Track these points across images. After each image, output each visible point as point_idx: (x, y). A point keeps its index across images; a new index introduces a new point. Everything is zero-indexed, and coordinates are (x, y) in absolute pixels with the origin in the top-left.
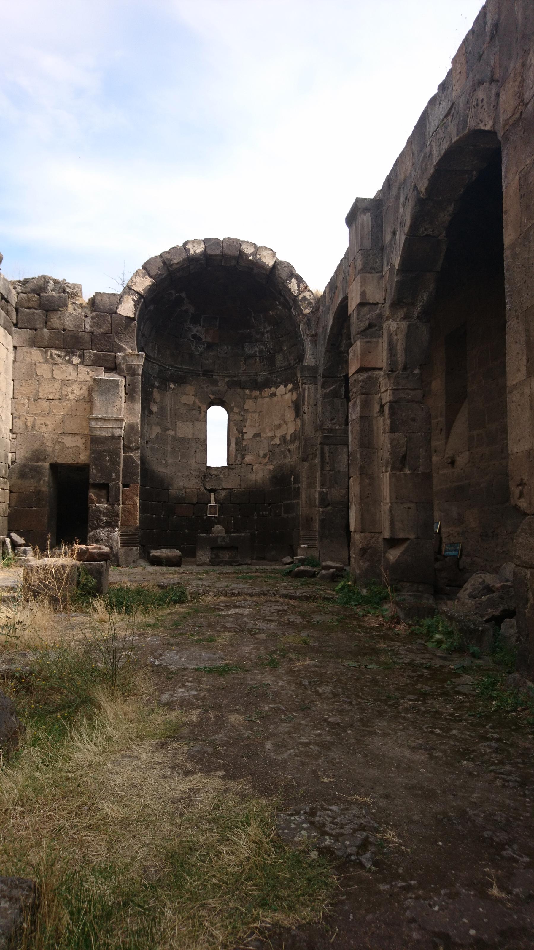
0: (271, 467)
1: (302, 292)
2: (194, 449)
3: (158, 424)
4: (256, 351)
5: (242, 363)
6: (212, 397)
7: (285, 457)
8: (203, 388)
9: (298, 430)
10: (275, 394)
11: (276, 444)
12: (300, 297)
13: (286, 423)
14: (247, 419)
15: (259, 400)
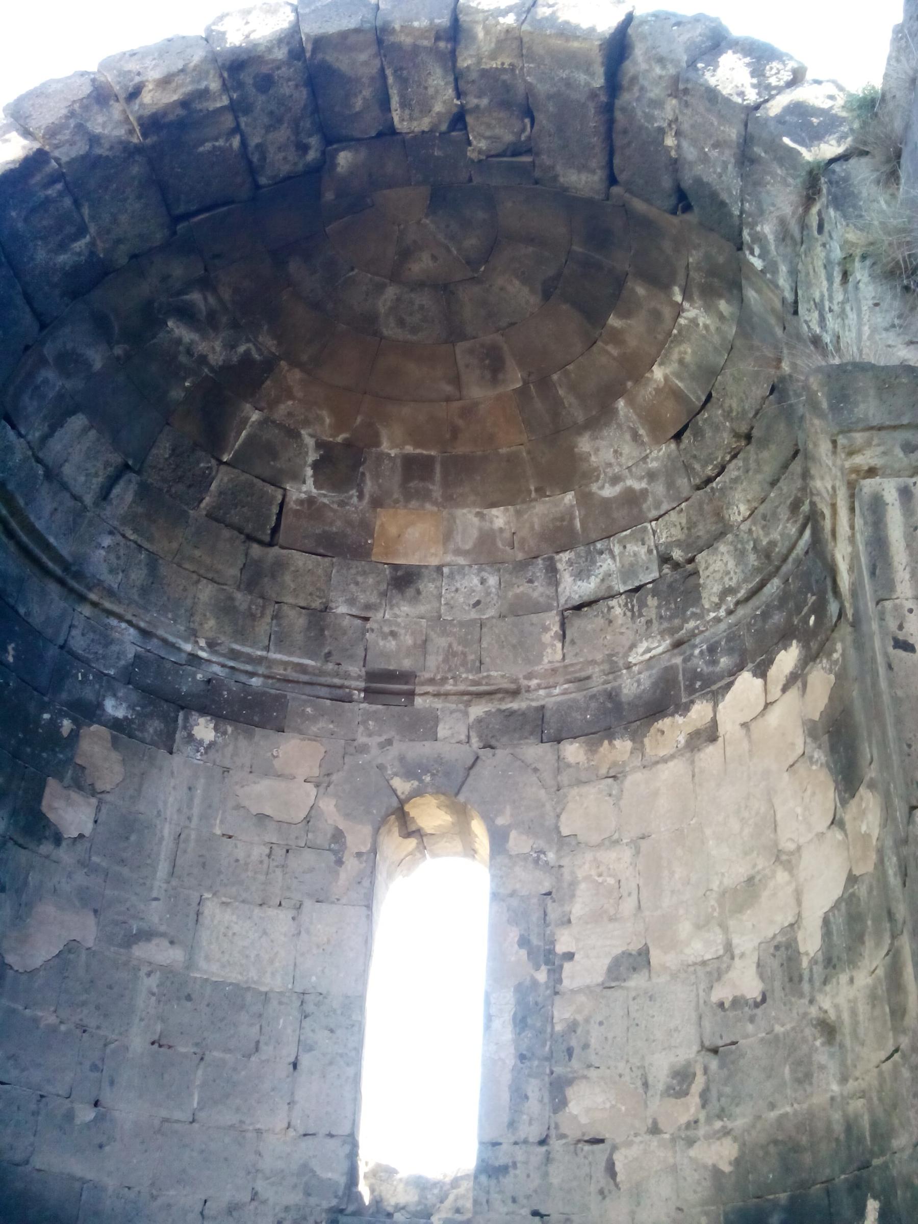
0: (722, 1154)
1: (780, 90)
2: (288, 1052)
3: (86, 900)
4: (608, 575)
5: (547, 638)
6: (402, 786)
7: (805, 1076)
8: (363, 749)
9: (866, 868)
10: (709, 734)
11: (737, 1002)
12: (776, 107)
13: (785, 859)
14: (573, 884)
15: (635, 780)
